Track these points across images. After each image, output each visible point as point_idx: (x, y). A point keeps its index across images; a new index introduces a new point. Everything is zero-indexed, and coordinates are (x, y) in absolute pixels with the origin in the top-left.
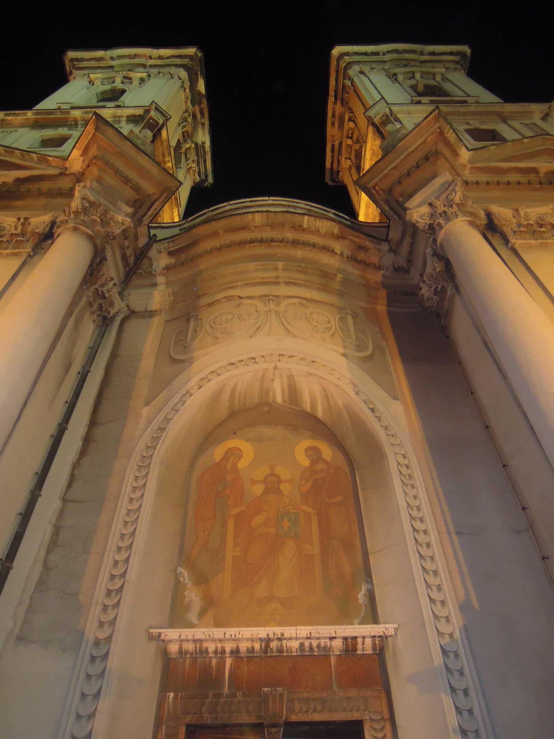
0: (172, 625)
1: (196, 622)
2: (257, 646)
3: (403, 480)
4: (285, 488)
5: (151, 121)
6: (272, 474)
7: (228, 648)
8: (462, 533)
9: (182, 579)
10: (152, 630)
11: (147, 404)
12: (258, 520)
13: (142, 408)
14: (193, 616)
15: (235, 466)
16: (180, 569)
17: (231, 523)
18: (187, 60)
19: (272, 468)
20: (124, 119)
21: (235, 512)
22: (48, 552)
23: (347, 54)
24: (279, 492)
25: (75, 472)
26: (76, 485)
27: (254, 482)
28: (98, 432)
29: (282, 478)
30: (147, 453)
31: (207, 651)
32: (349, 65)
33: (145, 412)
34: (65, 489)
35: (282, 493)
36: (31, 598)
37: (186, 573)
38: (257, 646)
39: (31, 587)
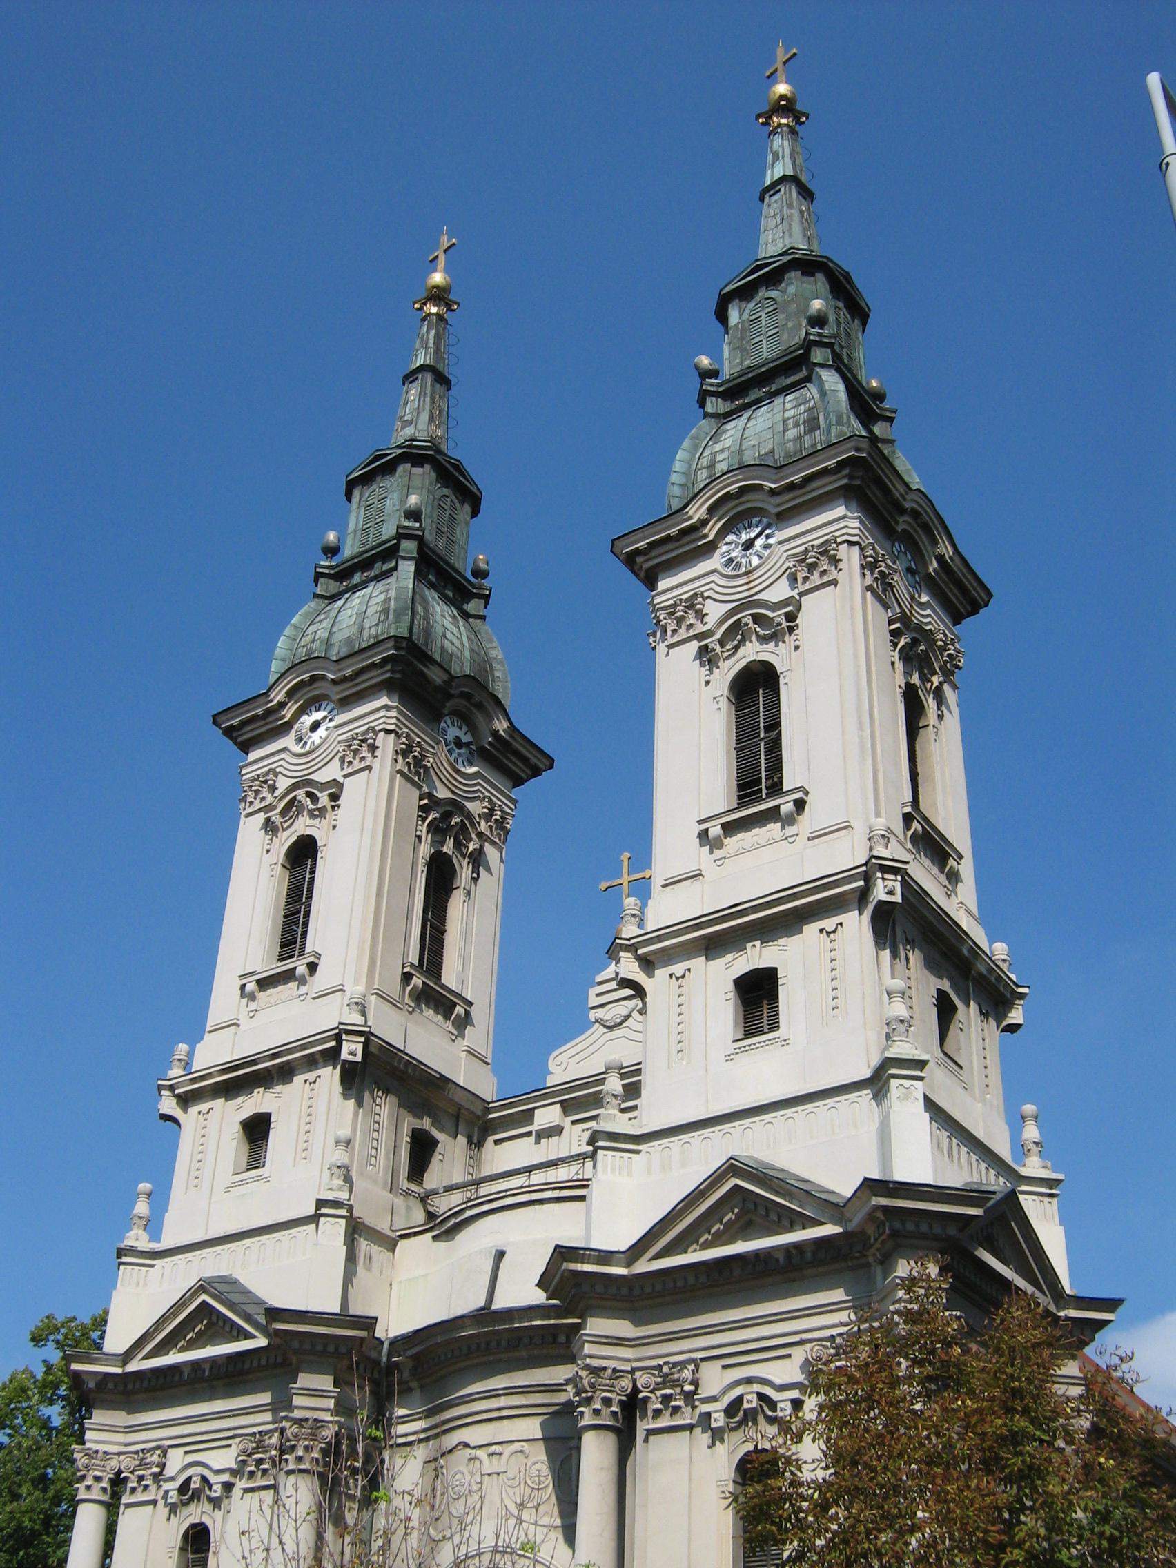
18: (389, 667)
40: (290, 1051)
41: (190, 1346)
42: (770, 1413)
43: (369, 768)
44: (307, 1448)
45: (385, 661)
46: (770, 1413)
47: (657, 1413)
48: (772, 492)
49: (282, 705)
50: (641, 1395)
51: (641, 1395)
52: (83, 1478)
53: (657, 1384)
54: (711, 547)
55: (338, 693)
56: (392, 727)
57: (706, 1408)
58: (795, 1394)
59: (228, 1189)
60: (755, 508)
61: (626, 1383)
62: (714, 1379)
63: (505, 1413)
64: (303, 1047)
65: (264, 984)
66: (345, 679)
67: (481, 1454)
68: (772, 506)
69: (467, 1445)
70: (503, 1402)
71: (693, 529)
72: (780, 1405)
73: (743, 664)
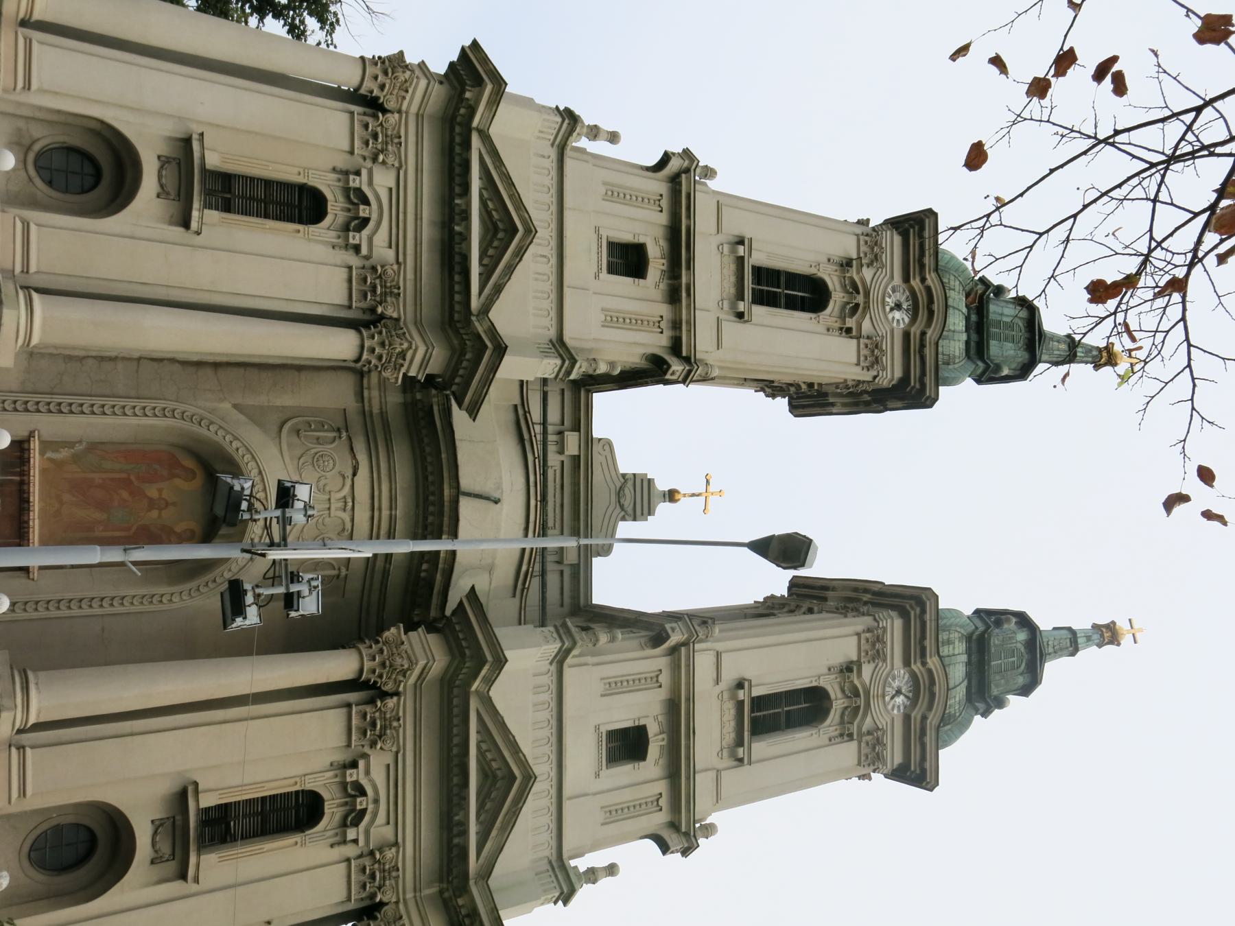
0: (41, 442)
1: (45, 457)
2: (26, 495)
3: (147, 597)
4: (155, 514)
5: (665, 367)
6: (167, 504)
7: (25, 478)
8: (103, 632)
9: (77, 445)
10: (36, 432)
11: (235, 406)
12: (125, 494)
13: (230, 402)
14: (49, 455)
15: (178, 476)
16: (84, 444)
17: (124, 475)
18: (918, 386)
19: (174, 504)
20: (678, 334)
21: (132, 477)
22: (95, 357)
23: (923, 611)
24: (150, 508)
25: (166, 361)
26: (155, 364)
27: (160, 491)
28: (209, 371)
29: (163, 511)
30: (178, 413)
31: (24, 465)
32: (904, 614)
33: (226, 406)
34: (149, 357)
35: (150, 511)
36: (58, 355)
37: (81, 447)
38: (26, 495)
39: (67, 352)
40: (689, 306)
41: (483, 202)
42: (353, 224)
43: (858, 364)
44: (380, 358)
45: (923, 385)
46: (353, 224)
47: (366, 126)
48: (924, 718)
49: (923, 280)
50: (380, 115)
51: (380, 115)
52: (377, 642)
53: (385, 282)
54: (907, 663)
55: (915, 334)
56: (877, 381)
57: (364, 172)
58: (364, 251)
59: (597, 230)
60: (918, 700)
61: (391, 104)
62: (383, 180)
63: (376, 514)
64: (688, 322)
65: (740, 261)
66: (922, 346)
67: (347, 489)
68: (916, 715)
69: (354, 474)
70: (385, 513)
71: (923, 654)
72: (357, 235)
73: (833, 696)
